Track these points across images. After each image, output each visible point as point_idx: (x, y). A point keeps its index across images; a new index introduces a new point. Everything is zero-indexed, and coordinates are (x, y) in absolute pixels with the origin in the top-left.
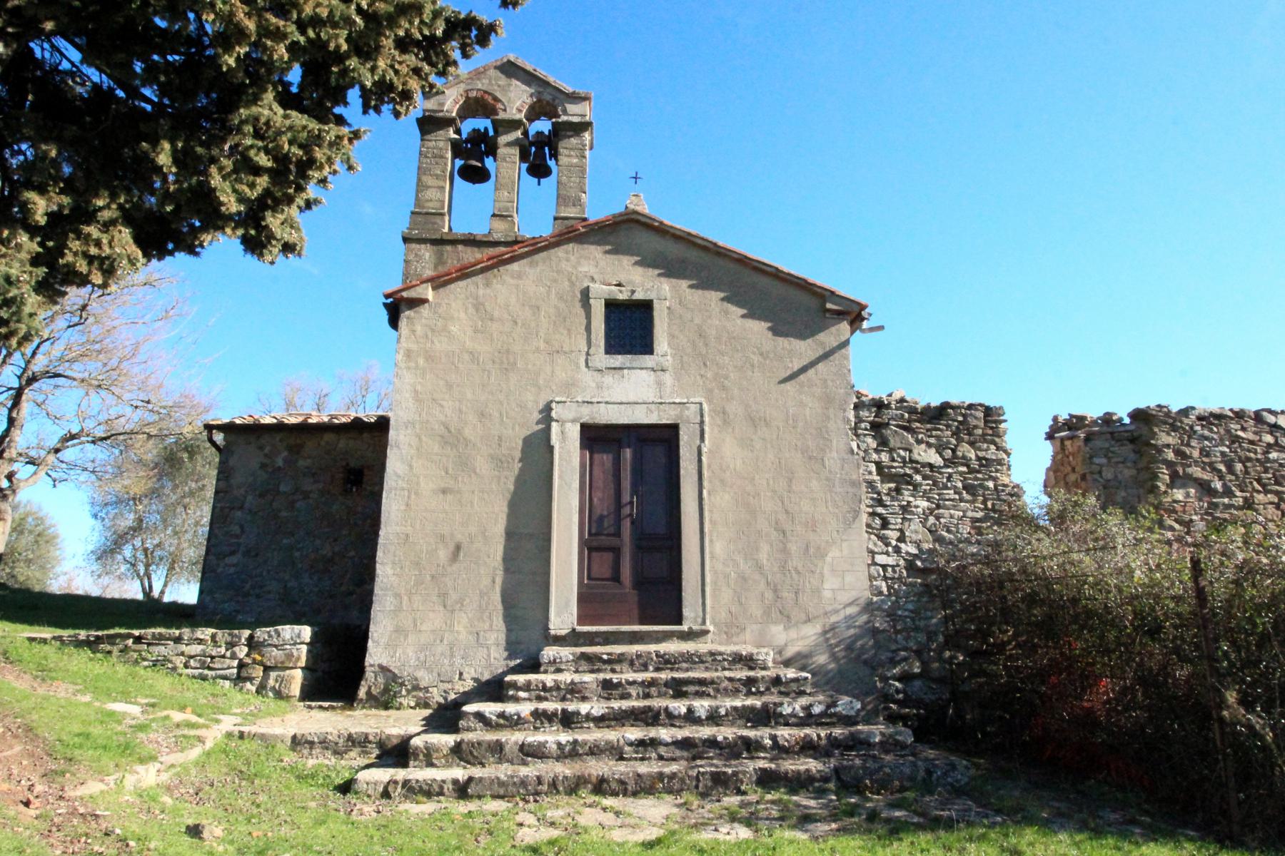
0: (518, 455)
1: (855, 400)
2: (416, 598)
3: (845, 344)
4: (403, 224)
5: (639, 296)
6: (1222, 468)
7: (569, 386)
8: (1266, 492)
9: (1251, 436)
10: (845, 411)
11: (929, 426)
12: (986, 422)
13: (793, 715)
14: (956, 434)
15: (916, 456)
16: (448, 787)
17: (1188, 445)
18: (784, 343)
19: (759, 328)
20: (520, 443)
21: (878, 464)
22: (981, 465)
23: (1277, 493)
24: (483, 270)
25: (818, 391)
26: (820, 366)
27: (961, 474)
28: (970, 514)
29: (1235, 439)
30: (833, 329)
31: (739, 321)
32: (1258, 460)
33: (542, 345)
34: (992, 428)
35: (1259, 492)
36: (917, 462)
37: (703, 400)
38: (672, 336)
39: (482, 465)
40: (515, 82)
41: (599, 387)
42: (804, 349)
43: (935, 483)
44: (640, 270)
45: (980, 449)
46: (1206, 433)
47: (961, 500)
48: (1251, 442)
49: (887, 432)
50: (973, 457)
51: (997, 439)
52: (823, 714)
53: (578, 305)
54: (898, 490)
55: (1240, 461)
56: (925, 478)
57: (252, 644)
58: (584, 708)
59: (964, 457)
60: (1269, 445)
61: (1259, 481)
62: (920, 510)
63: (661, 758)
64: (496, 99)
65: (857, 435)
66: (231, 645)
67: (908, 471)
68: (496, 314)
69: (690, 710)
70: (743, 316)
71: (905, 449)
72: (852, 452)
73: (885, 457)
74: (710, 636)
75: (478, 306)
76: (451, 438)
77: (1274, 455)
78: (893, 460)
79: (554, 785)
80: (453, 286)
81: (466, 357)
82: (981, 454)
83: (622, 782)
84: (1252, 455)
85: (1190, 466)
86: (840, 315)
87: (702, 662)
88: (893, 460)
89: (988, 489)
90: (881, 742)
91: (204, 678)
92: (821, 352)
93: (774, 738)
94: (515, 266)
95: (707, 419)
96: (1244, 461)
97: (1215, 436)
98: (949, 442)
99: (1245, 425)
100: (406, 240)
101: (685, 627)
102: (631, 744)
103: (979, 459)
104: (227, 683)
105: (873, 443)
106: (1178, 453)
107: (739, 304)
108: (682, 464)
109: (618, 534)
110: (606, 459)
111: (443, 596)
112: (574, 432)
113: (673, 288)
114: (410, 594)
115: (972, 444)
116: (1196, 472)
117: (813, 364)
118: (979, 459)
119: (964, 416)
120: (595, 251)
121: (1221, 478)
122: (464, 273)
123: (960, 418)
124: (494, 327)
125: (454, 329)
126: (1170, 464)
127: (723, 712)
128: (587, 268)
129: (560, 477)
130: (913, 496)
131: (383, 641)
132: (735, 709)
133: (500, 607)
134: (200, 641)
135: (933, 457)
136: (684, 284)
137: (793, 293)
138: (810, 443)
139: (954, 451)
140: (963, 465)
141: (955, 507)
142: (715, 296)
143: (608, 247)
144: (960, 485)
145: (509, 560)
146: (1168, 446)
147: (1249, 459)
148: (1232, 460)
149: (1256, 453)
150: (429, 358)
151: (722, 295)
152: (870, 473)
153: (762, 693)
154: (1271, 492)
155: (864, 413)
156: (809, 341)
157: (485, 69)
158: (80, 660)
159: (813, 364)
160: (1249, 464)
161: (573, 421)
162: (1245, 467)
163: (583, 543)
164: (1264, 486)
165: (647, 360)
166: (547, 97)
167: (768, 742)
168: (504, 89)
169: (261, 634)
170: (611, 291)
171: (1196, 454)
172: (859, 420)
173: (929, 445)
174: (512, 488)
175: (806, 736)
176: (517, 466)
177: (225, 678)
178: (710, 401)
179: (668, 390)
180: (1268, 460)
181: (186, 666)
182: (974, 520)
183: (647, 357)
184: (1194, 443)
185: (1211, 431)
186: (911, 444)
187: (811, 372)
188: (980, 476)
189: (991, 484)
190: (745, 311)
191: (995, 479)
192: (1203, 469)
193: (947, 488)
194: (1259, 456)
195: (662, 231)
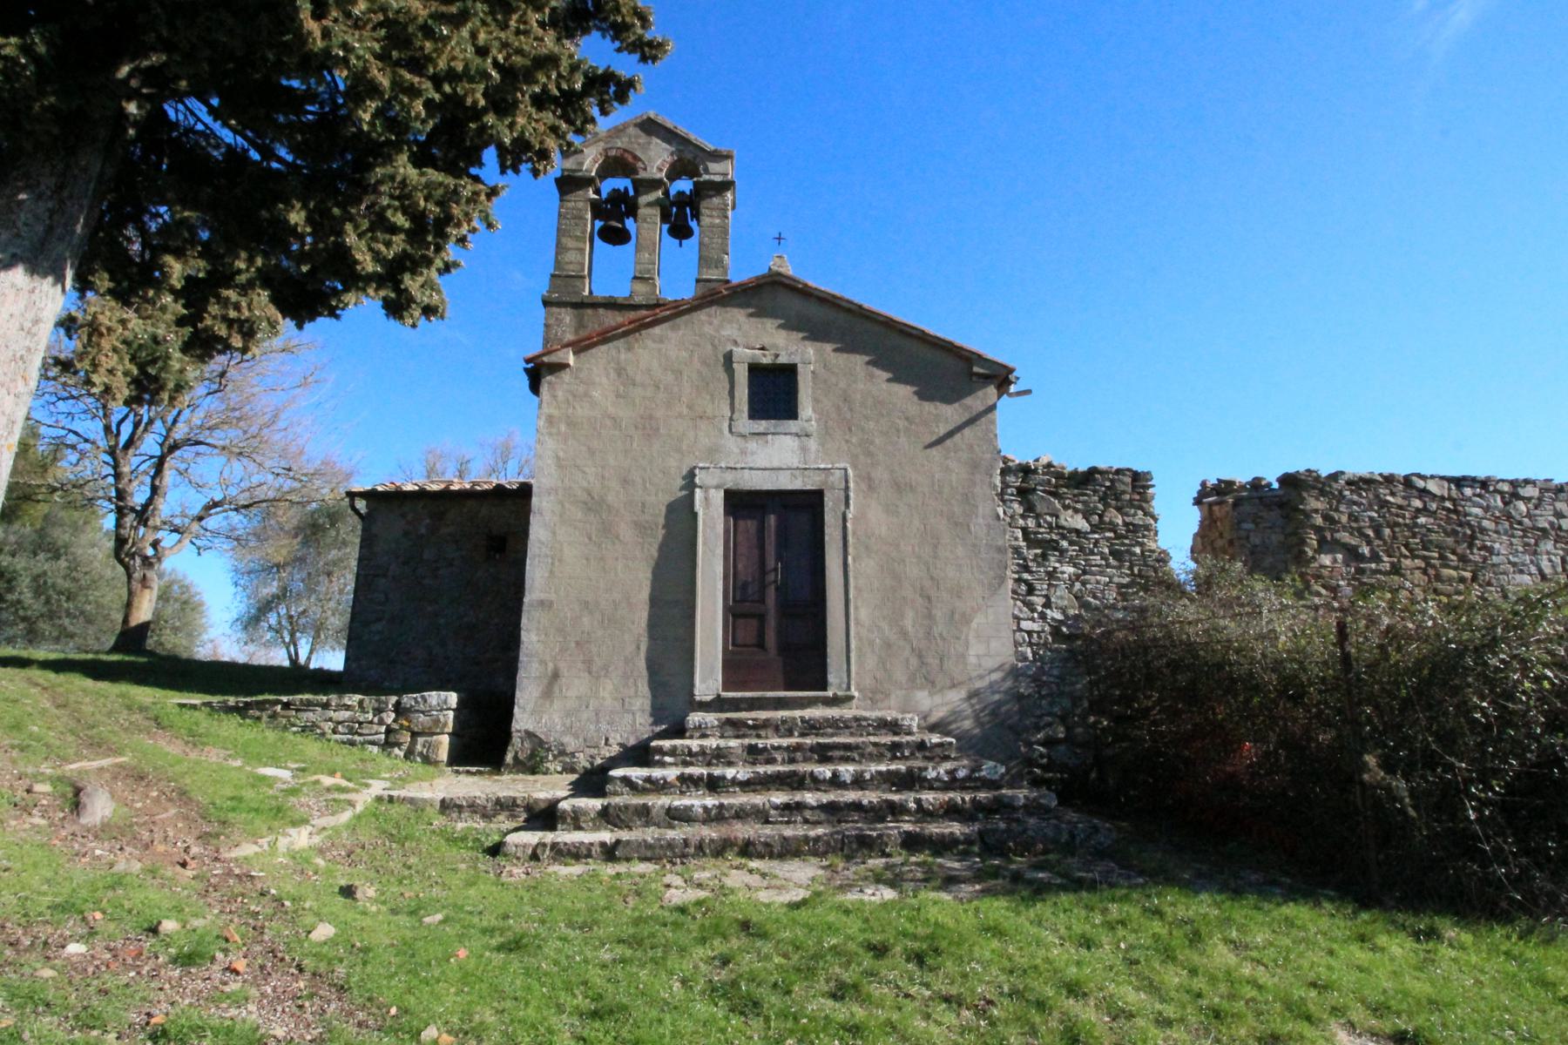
0: (662, 521)
1: (1001, 465)
3: (992, 408)
4: (542, 286)
5: (783, 360)
6: (1371, 533)
7: (713, 452)
8: (1414, 557)
9: (1399, 501)
10: (991, 476)
11: (1076, 491)
12: (1134, 487)
13: (937, 779)
15: (1062, 522)
16: (596, 850)
17: (1337, 510)
18: (928, 407)
19: (904, 391)
20: (664, 509)
21: (1025, 530)
22: (1128, 531)
23: (1424, 558)
24: (625, 334)
25: (965, 456)
26: (967, 431)
27: (1108, 539)
28: (1116, 580)
29: (1384, 504)
30: (980, 393)
31: (885, 386)
32: (1406, 525)
33: (685, 411)
34: (1139, 493)
35: (1406, 557)
37: (848, 466)
38: (816, 401)
39: (626, 531)
40: (656, 140)
41: (743, 452)
42: (949, 414)
43: (1082, 549)
44: (783, 333)
45: (1128, 516)
46: (1355, 497)
47: (1108, 566)
48: (1400, 507)
50: (1120, 521)
51: (1144, 505)
52: (964, 780)
53: (721, 369)
54: (1044, 556)
55: (1388, 526)
56: (1071, 543)
57: (398, 709)
58: (730, 773)
59: (1111, 523)
60: (1418, 510)
61: (1406, 546)
62: (1066, 576)
63: (806, 821)
64: (636, 158)
65: (1004, 501)
66: (378, 711)
67: (1054, 537)
68: (638, 379)
69: (835, 775)
70: (889, 380)
71: (1051, 515)
72: (998, 517)
73: (1031, 523)
74: (855, 701)
75: (620, 371)
76: (594, 504)
77: (1422, 520)
78: (1039, 525)
79: (700, 848)
80: (594, 351)
81: (608, 422)
82: (1128, 519)
83: (767, 845)
84: (1401, 520)
85: (1338, 531)
86: (986, 379)
87: (847, 727)
88: (1039, 525)
89: (1134, 554)
90: (1025, 806)
91: (352, 743)
92: (966, 416)
93: (918, 802)
94: (657, 330)
95: (852, 485)
96: (1392, 526)
97: (1364, 501)
98: (1096, 508)
99: (1394, 490)
101: (830, 693)
102: (776, 807)
103: (1126, 524)
104: (375, 749)
105: (1018, 508)
106: (1326, 517)
107: (884, 368)
108: (827, 530)
109: (762, 601)
110: (750, 525)
111: (588, 663)
112: (718, 498)
113: (817, 351)
115: (1119, 509)
116: (1344, 537)
117: (959, 429)
118: (1126, 524)
119: (1112, 481)
120: (739, 314)
121: (1369, 543)
122: (606, 337)
123: (1108, 484)
125: (596, 394)
126: (1318, 530)
127: (867, 776)
128: (729, 331)
129: (704, 544)
130: (1059, 561)
131: (529, 707)
132: (880, 773)
133: (645, 673)
134: (348, 708)
135: (1080, 523)
136: (828, 347)
139: (1101, 516)
140: (1110, 530)
141: (1102, 573)
142: (859, 360)
143: (751, 310)
145: (655, 625)
146: (1316, 511)
147: (1398, 524)
148: (1380, 526)
149: (1404, 517)
150: (571, 424)
151: (867, 358)
153: (907, 758)
154: (1418, 557)
155: (1011, 479)
156: (956, 405)
157: (625, 127)
158: (230, 726)
159: (959, 429)
160: (1397, 529)
161: (717, 487)
162: (1393, 532)
163: (727, 610)
164: (1411, 551)
165: (792, 425)
166: (689, 156)
167: (912, 805)
168: (645, 147)
169: (408, 700)
170: (755, 355)
171: (1344, 519)
172: (1005, 485)
173: (1076, 511)
174: (656, 554)
175: (951, 799)
176: (661, 533)
177: (373, 743)
178: (855, 467)
179: (813, 456)
180: (1416, 525)
181: (335, 732)
182: (1120, 586)
184: (1343, 508)
185: (1360, 496)
187: (958, 437)
188: (1127, 541)
190: (890, 375)
191: (1142, 545)
192: (1351, 534)
193: (1093, 554)
194: (1407, 521)
195: (806, 293)
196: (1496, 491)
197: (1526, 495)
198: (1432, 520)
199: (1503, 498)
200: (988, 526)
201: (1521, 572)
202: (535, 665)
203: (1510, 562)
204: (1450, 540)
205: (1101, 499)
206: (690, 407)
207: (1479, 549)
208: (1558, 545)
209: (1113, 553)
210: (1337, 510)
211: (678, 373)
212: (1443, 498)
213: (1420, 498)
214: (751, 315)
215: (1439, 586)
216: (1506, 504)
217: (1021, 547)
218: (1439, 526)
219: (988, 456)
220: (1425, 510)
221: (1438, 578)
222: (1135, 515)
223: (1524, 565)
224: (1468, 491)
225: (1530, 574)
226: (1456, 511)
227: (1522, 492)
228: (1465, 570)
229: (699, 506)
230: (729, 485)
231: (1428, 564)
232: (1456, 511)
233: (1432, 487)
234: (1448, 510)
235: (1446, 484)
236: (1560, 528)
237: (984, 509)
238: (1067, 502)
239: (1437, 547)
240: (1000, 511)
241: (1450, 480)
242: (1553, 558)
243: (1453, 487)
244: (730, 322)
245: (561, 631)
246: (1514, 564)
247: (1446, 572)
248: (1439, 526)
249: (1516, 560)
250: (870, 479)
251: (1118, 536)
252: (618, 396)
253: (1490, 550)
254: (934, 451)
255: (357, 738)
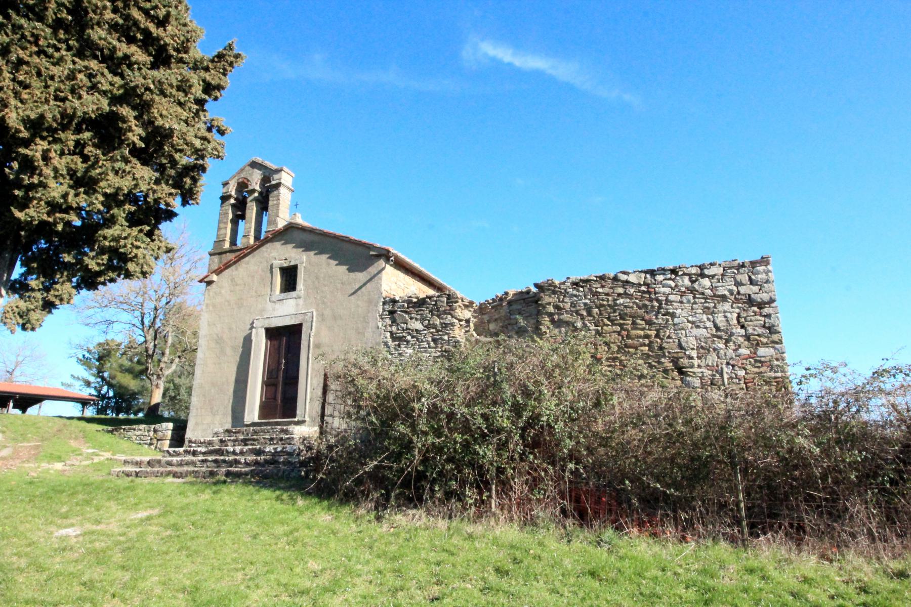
0: (241, 345)
1: (383, 300)
2: (203, 410)
3: (383, 269)
4: (210, 248)
5: (292, 264)
6: (585, 313)
7: (263, 310)
8: (613, 324)
9: (606, 290)
10: (377, 306)
11: (417, 309)
12: (447, 303)
13: (269, 452)
14: (431, 311)
15: (409, 327)
16: (134, 474)
17: (563, 301)
18: (352, 275)
19: (344, 268)
20: (242, 339)
21: (391, 332)
22: (442, 327)
23: (621, 325)
24: (235, 263)
25: (366, 298)
26: (368, 285)
27: (432, 333)
28: (433, 354)
29: (596, 294)
30: (376, 264)
31: (334, 268)
32: (609, 305)
33: (254, 294)
34: (450, 306)
35: (608, 325)
36: (409, 329)
37: (314, 310)
38: (304, 280)
39: (229, 351)
40: (256, 170)
41: (274, 310)
42: (361, 277)
43: (418, 340)
44: (295, 250)
45: (442, 319)
46: (575, 292)
47: (430, 347)
48: (607, 294)
49: (396, 315)
50: (438, 323)
51: (452, 312)
52: (281, 451)
53: (269, 272)
54: (399, 346)
55: (597, 307)
56: (413, 337)
57: (155, 431)
58: (199, 449)
59: (433, 324)
60: (619, 295)
61: (608, 319)
62: (408, 355)
63: (207, 467)
64: (248, 181)
65: (382, 319)
66: (149, 431)
67: (404, 335)
68: (238, 282)
69: (234, 450)
70: (336, 265)
71: (404, 323)
72: (378, 327)
73: (394, 329)
74: (307, 423)
75: (232, 280)
76: (219, 340)
77: (621, 301)
78: (398, 330)
79: (162, 474)
80: (224, 273)
81: (226, 303)
82: (442, 321)
83: (181, 473)
84: (605, 303)
85: (563, 314)
86: (378, 256)
87: (268, 432)
88: (398, 330)
89: (444, 340)
90: (283, 462)
91: (140, 444)
92: (369, 277)
93: (245, 459)
94: (247, 259)
95: (315, 319)
96: (599, 307)
97: (581, 294)
98: (427, 317)
99: (604, 284)
100: (211, 254)
101: (296, 420)
102: (199, 461)
103: (441, 324)
104: (146, 446)
105: (389, 322)
106: (557, 307)
107: (335, 259)
108: (302, 342)
109: (277, 377)
110: (276, 343)
111: (212, 409)
112: (262, 333)
113: (308, 256)
114: (201, 408)
115: (438, 316)
116: (565, 317)
117: (365, 284)
118: (441, 324)
119: (436, 301)
120: (277, 245)
121: (583, 318)
122: (227, 266)
123: (433, 303)
124: (238, 288)
125: (223, 291)
126: (551, 315)
127: (245, 450)
128: (274, 254)
129: (254, 354)
130: (406, 347)
131: (192, 428)
132: (249, 449)
133: (230, 413)
134: (140, 430)
135: (418, 325)
136: (312, 253)
137: (360, 249)
138: (359, 325)
139: (429, 321)
140: (433, 328)
141: (425, 352)
142: (324, 257)
143: (283, 242)
144: (430, 339)
145: (235, 392)
146: (549, 304)
147: (603, 306)
148: (591, 307)
149: (608, 301)
150: (214, 306)
151: (328, 256)
152: (386, 338)
153: (275, 444)
154: (616, 325)
155: (387, 307)
156: (364, 272)
157: (245, 167)
158: (108, 438)
159: (365, 284)
160: (602, 309)
161: (262, 327)
162: (600, 311)
163: (263, 382)
164: (612, 321)
165: (293, 294)
166: (267, 174)
167: (243, 461)
168: (251, 175)
169: (157, 426)
170: (281, 264)
171: (568, 306)
172: (384, 310)
173: (417, 319)
174: (238, 360)
175: (256, 459)
176: (241, 350)
177: (146, 444)
178: (317, 310)
179: (300, 307)
180: (616, 305)
181: (136, 439)
182: (435, 357)
183: (293, 293)
184: (567, 300)
185: (578, 291)
186: (407, 320)
187: (363, 289)
188: (440, 333)
189: (446, 337)
190: (337, 262)
191: (448, 334)
192: (572, 315)
193: (423, 342)
194: (610, 303)
195: (303, 229)
196: (684, 274)
197: (711, 273)
198: (628, 300)
199: (690, 278)
200: (374, 332)
201: (698, 327)
202: (195, 411)
203: (689, 321)
204: (641, 312)
205: (430, 311)
206: (256, 292)
207: (663, 315)
208: (734, 305)
209: (434, 340)
210: (563, 301)
211: (253, 277)
212: (639, 285)
213: (623, 287)
214: (283, 244)
215: (630, 341)
216: (693, 282)
217: (387, 342)
218: (634, 303)
219: (377, 296)
220: (626, 295)
221: (628, 337)
222: (446, 318)
223: (700, 322)
224: (660, 278)
225: (706, 328)
226: (649, 293)
227: (706, 272)
228: (650, 330)
229: (253, 338)
230: (267, 326)
231: (622, 329)
232: (649, 293)
233: (632, 278)
234: (644, 292)
235: (643, 275)
236: (739, 293)
237: (372, 325)
238: (413, 315)
239: (630, 317)
240: (380, 324)
241: (646, 272)
242: (728, 315)
243: (648, 276)
244: (274, 249)
245: (204, 395)
246: (693, 323)
247: (634, 332)
248: (634, 303)
249: (694, 319)
250: (323, 315)
251: (438, 331)
252: (231, 291)
253: (673, 315)
254: (352, 297)
255: (142, 442)
